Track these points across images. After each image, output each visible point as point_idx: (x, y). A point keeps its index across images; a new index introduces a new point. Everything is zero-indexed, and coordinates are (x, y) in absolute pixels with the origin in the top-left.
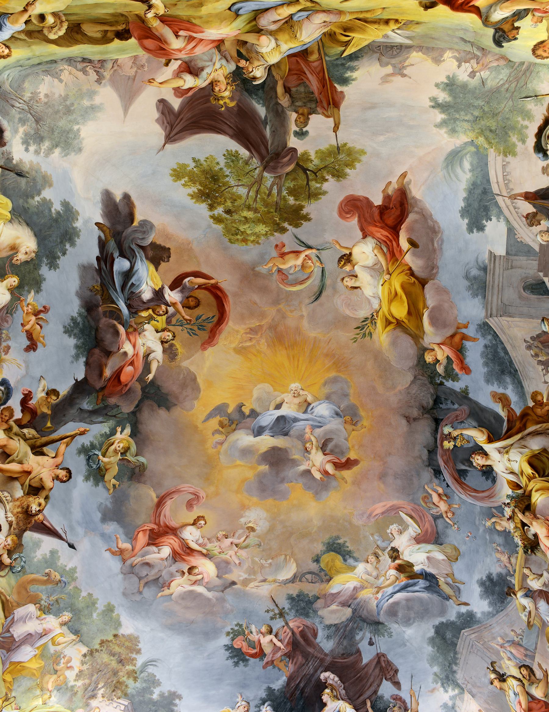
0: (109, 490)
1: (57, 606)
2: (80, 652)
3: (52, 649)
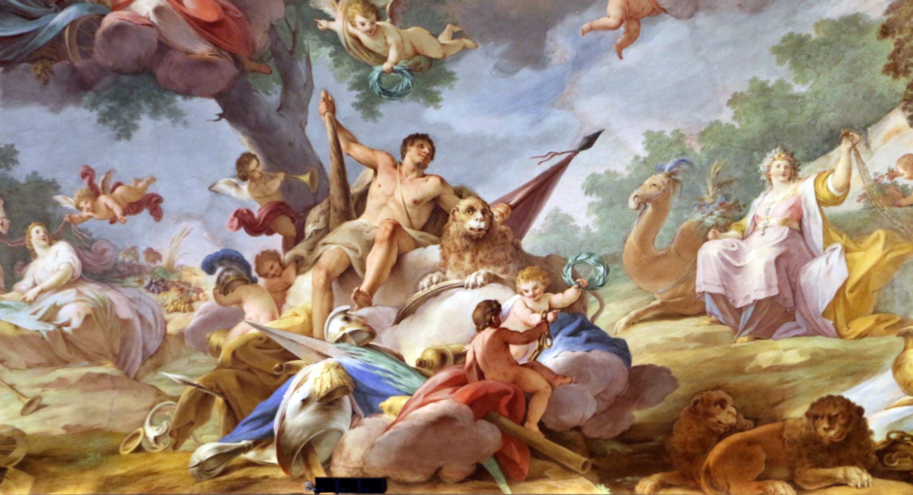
0: (465, 49)
1: (735, 185)
2: (898, 131)
3: (852, 205)
